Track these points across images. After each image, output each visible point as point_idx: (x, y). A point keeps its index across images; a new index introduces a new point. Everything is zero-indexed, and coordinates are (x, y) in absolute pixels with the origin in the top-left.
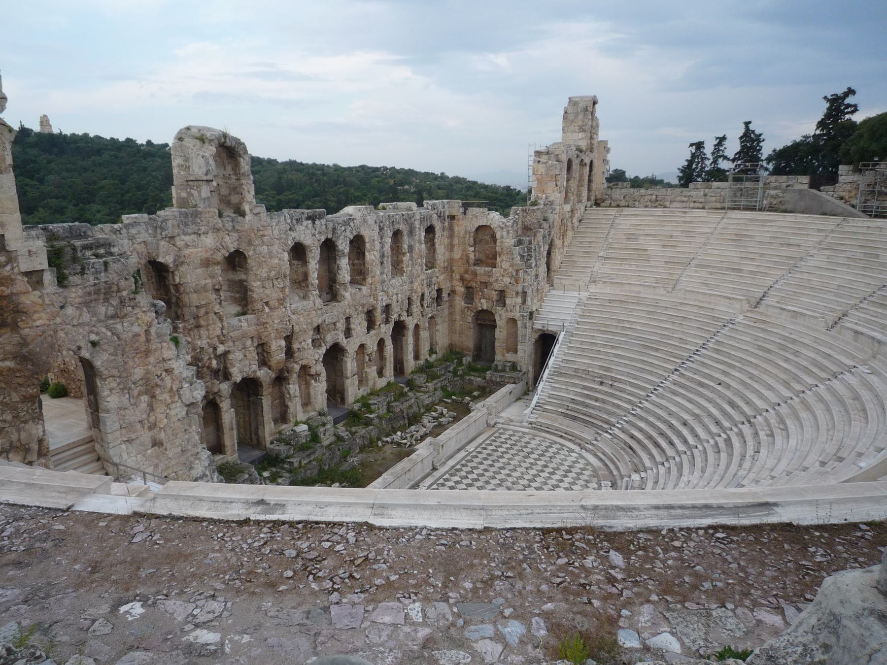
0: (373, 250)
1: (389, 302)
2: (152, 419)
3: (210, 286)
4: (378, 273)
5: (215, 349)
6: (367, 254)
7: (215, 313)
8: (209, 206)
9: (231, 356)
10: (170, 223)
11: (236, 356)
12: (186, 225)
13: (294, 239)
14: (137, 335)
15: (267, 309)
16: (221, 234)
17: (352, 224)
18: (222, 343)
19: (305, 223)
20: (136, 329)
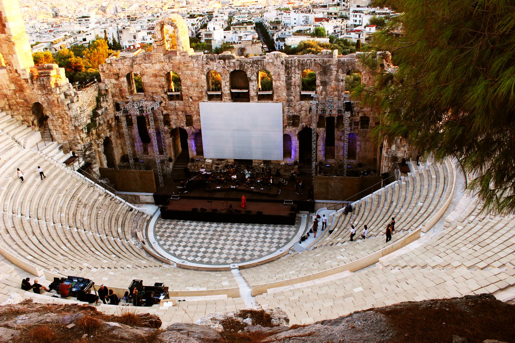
0: (279, 80)
1: (296, 114)
2: (63, 126)
3: (157, 85)
4: (285, 94)
5: (162, 111)
6: (273, 82)
7: (163, 97)
8: (156, 52)
9: (170, 117)
10: (138, 59)
11: (173, 117)
12: (145, 60)
13: (208, 69)
14: (53, 101)
15: (191, 100)
16: (164, 64)
17: (259, 63)
18: (166, 110)
19: (217, 61)
20: (54, 99)
